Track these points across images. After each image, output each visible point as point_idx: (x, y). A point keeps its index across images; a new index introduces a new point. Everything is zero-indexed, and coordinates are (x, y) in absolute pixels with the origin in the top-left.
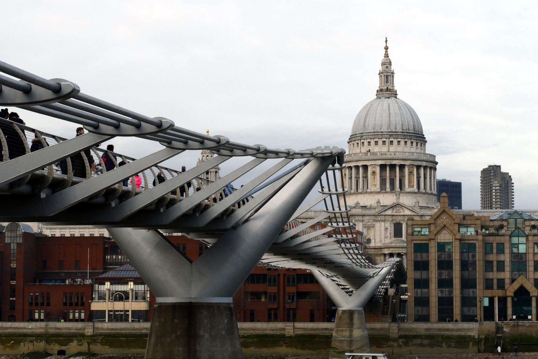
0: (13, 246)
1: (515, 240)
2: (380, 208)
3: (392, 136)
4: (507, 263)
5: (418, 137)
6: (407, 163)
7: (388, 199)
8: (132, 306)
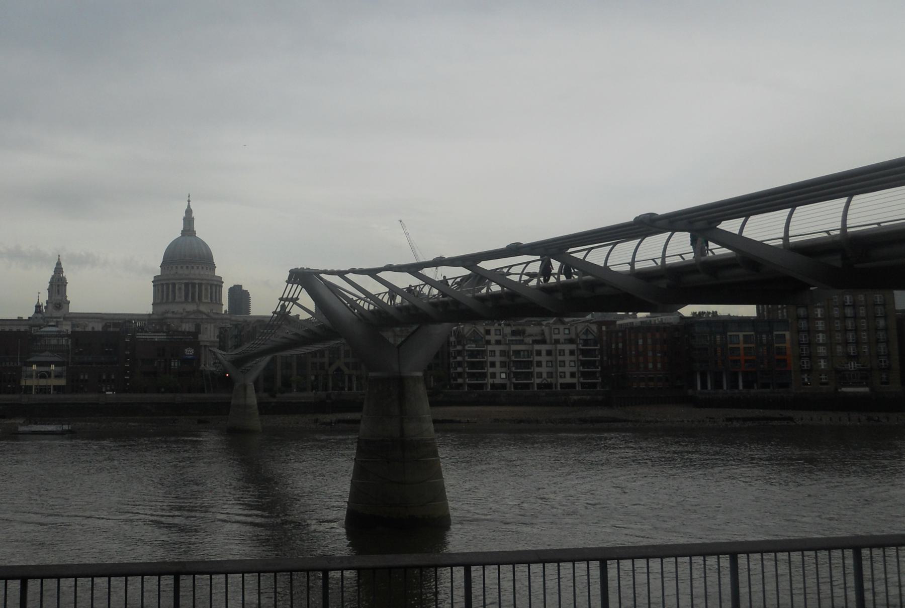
2: (185, 314)
6: (204, 282)
7: (191, 307)
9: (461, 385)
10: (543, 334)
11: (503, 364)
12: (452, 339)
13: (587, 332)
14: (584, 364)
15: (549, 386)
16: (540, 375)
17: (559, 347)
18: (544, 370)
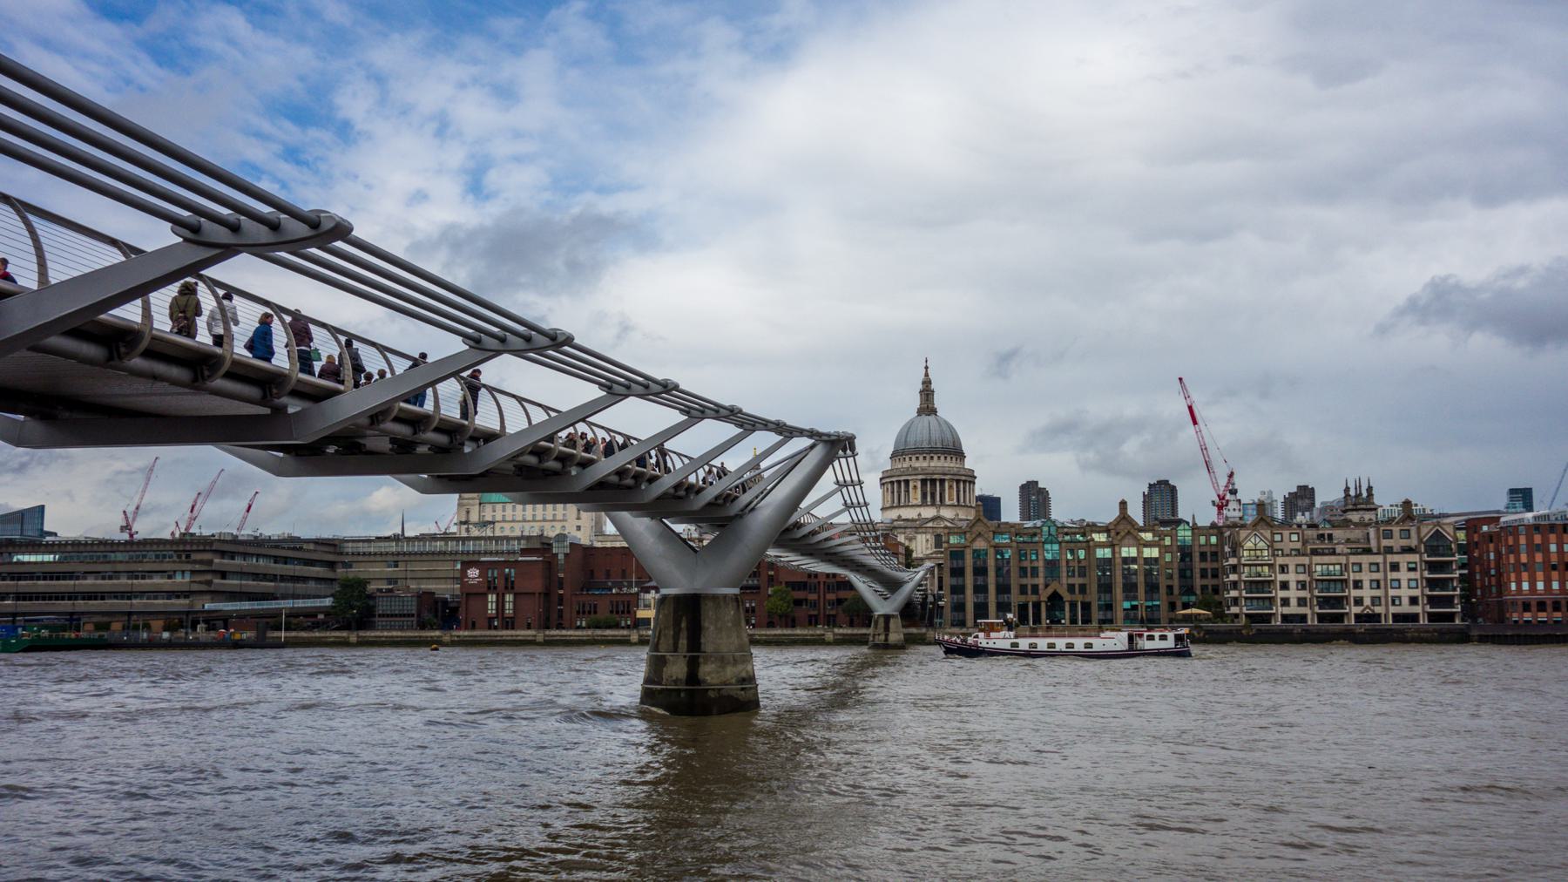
0: (561, 557)
1: (1048, 546)
3: (932, 452)
4: (1041, 570)
5: (958, 454)
7: (928, 513)
9: (1236, 616)
11: (1302, 585)
12: (1227, 549)
14: (1432, 584)
15: (1375, 617)
16: (1359, 601)
17: (1391, 558)
18: (1367, 593)
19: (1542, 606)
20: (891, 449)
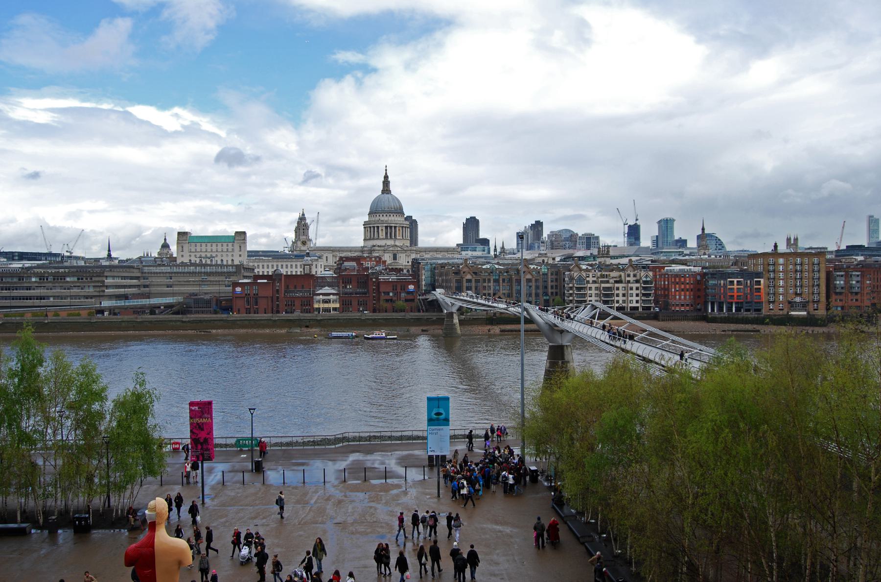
5: (399, 211)
7: (390, 242)
8: (331, 306)
10: (620, 276)
12: (566, 279)
13: (647, 276)
17: (630, 285)
19: (683, 305)
20: (368, 211)
